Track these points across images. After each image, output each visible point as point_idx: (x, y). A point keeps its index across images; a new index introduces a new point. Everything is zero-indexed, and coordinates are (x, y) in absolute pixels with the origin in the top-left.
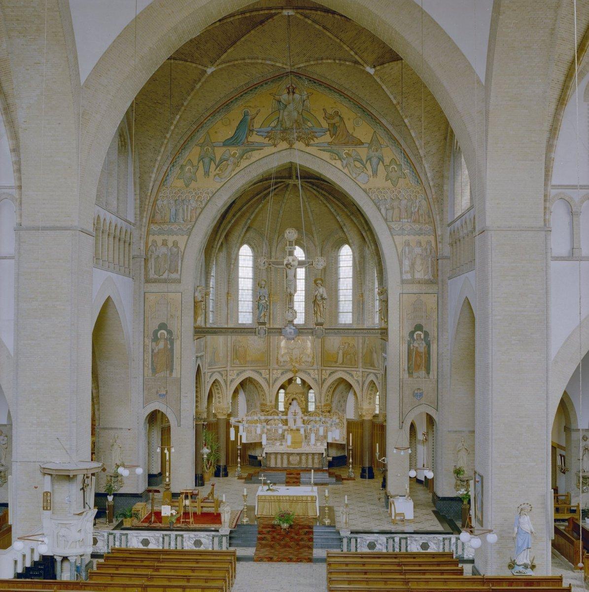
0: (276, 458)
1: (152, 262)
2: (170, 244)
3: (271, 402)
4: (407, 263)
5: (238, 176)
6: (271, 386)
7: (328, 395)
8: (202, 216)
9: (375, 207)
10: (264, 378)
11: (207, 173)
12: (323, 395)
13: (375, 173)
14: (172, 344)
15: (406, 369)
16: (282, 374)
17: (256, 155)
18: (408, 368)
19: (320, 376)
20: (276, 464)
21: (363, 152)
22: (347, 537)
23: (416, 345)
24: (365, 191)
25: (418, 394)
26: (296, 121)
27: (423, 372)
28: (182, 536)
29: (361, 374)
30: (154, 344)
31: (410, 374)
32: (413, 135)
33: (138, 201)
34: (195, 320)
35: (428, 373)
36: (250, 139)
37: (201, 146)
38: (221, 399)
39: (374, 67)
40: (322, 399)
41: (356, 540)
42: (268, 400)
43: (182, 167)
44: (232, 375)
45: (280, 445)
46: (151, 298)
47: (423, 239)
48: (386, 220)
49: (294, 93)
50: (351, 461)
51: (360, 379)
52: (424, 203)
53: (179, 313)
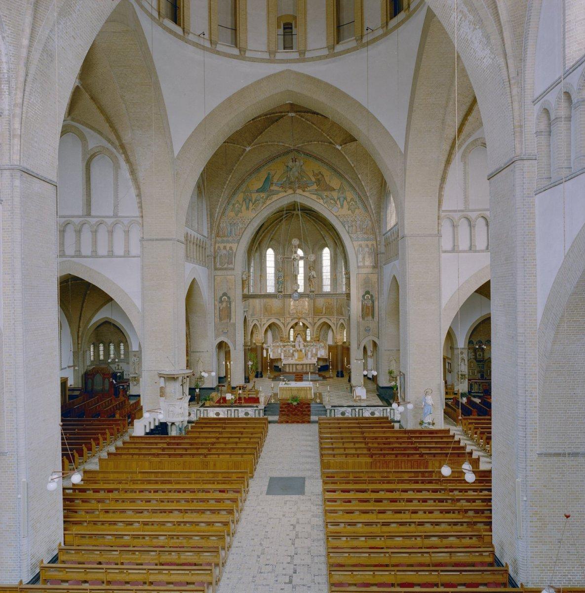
0: (289, 367)
1: (218, 259)
2: (228, 248)
4: (360, 256)
5: (265, 209)
8: (245, 232)
9: (342, 226)
11: (248, 208)
12: (315, 331)
13: (342, 206)
14: (230, 304)
15: (361, 315)
16: (292, 320)
17: (275, 198)
18: (362, 315)
20: (289, 370)
21: (335, 194)
22: (329, 409)
23: (366, 302)
24: (336, 216)
25: (367, 330)
26: (297, 177)
27: (370, 317)
28: (238, 410)
29: (335, 319)
30: (220, 304)
31: (363, 318)
32: (363, 184)
33: (209, 224)
34: (243, 291)
35: (373, 318)
36: (272, 188)
37: (244, 192)
39: (341, 145)
41: (335, 411)
43: (234, 205)
44: (264, 321)
46: (218, 279)
47: (370, 243)
48: (348, 233)
49: (295, 161)
50: (331, 367)
51: (335, 322)
52: (370, 222)
53: (234, 286)
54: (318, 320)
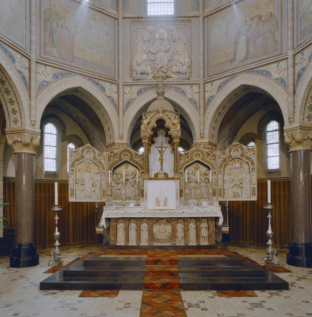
0: (127, 230)
3: (121, 138)
6: (121, 113)
16: (140, 92)
19: (202, 94)
20: (127, 240)
38: (18, 114)
40: (207, 132)
42: (117, 136)
45: (135, 205)
50: (270, 232)
54: (220, 87)
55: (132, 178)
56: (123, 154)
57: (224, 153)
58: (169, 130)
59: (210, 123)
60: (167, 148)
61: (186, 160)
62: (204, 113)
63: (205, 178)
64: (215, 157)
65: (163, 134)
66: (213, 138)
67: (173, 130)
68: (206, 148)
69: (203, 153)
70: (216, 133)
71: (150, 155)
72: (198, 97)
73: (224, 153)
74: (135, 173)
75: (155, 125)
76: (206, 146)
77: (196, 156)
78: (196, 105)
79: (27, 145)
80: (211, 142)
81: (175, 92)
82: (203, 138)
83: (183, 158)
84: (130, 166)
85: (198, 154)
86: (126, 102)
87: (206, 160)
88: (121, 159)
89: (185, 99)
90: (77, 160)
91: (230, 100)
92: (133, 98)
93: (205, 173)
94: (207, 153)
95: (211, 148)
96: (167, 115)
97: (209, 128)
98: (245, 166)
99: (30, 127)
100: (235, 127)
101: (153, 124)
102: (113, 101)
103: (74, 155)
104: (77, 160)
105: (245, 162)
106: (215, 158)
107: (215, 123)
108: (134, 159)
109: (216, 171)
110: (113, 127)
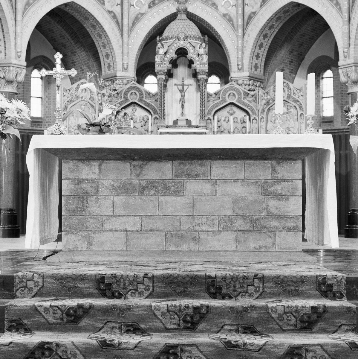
3: (126, 69)
7: (261, 46)
10: (110, 12)
19: (240, 9)
40: (246, 62)
42: (119, 66)
55: (142, 126)
56: (130, 92)
57: (267, 93)
58: (193, 63)
59: (250, 50)
60: (190, 86)
61: (216, 102)
62: (244, 35)
63: (242, 126)
64: (256, 97)
65: (184, 64)
66: (256, 70)
67: (198, 63)
68: (245, 85)
69: (239, 93)
70: (261, 62)
71: (166, 94)
72: (236, 12)
73: (267, 93)
74: (146, 119)
75: (175, 56)
76: (245, 82)
77: (230, 97)
78: (231, 22)
79: (10, 82)
80: (252, 75)
81: (202, 5)
82: (242, 71)
83: (212, 99)
84: (139, 109)
85: (233, 93)
86: (133, 17)
87: (244, 102)
88: (126, 100)
89: (218, 15)
90: (71, 101)
91: (279, 18)
92: (142, 12)
93: (242, 120)
94: (244, 92)
95: (253, 84)
96: (190, 43)
97: (250, 57)
98: (292, 110)
99: (16, 59)
100: (299, 47)
101: (172, 55)
102: (114, 17)
103: (67, 95)
104: (71, 101)
105: (293, 106)
106: (256, 99)
107: (260, 49)
108: (145, 100)
109: (257, 118)
110: (114, 54)
